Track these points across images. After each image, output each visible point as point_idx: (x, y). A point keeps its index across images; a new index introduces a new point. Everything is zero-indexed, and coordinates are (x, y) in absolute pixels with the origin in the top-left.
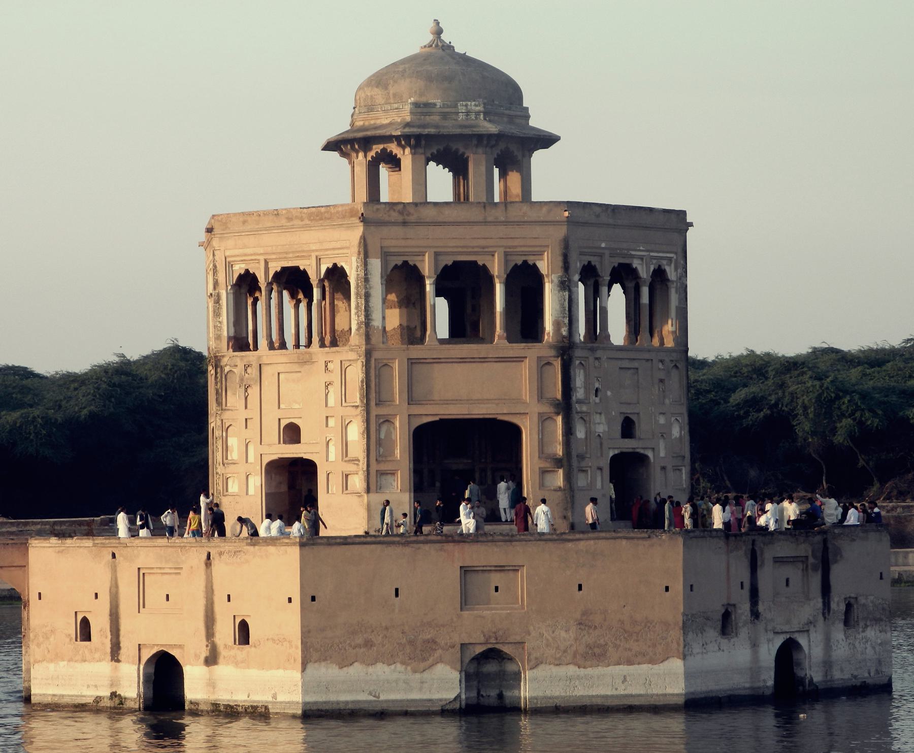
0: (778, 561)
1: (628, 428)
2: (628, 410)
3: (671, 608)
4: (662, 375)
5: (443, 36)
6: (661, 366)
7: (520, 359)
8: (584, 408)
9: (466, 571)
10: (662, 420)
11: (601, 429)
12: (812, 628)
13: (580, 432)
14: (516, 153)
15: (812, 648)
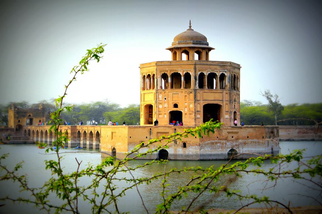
0: (158, 133)
1: (176, 106)
2: (175, 102)
3: (126, 142)
4: (187, 95)
5: (191, 28)
6: (186, 93)
7: (152, 93)
8: (161, 102)
9: (112, 133)
10: (186, 104)
11: (166, 106)
12: (170, 147)
13: (161, 106)
14: (188, 50)
15: (171, 151)
